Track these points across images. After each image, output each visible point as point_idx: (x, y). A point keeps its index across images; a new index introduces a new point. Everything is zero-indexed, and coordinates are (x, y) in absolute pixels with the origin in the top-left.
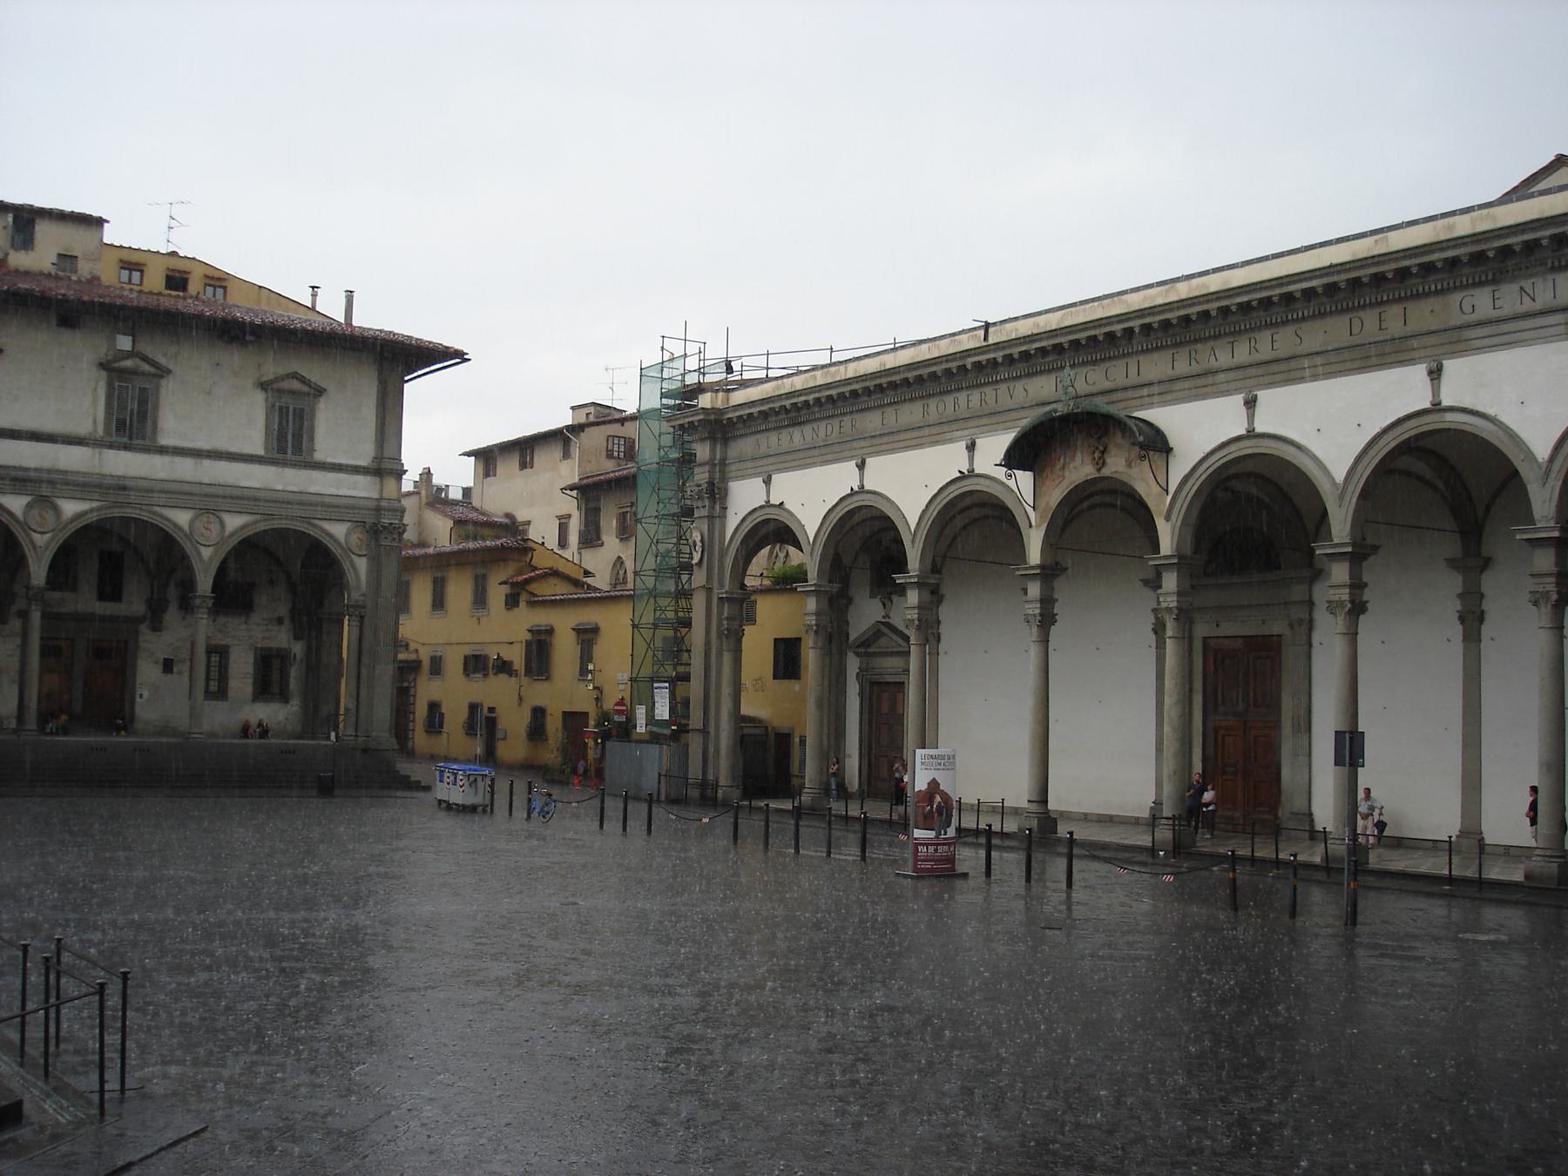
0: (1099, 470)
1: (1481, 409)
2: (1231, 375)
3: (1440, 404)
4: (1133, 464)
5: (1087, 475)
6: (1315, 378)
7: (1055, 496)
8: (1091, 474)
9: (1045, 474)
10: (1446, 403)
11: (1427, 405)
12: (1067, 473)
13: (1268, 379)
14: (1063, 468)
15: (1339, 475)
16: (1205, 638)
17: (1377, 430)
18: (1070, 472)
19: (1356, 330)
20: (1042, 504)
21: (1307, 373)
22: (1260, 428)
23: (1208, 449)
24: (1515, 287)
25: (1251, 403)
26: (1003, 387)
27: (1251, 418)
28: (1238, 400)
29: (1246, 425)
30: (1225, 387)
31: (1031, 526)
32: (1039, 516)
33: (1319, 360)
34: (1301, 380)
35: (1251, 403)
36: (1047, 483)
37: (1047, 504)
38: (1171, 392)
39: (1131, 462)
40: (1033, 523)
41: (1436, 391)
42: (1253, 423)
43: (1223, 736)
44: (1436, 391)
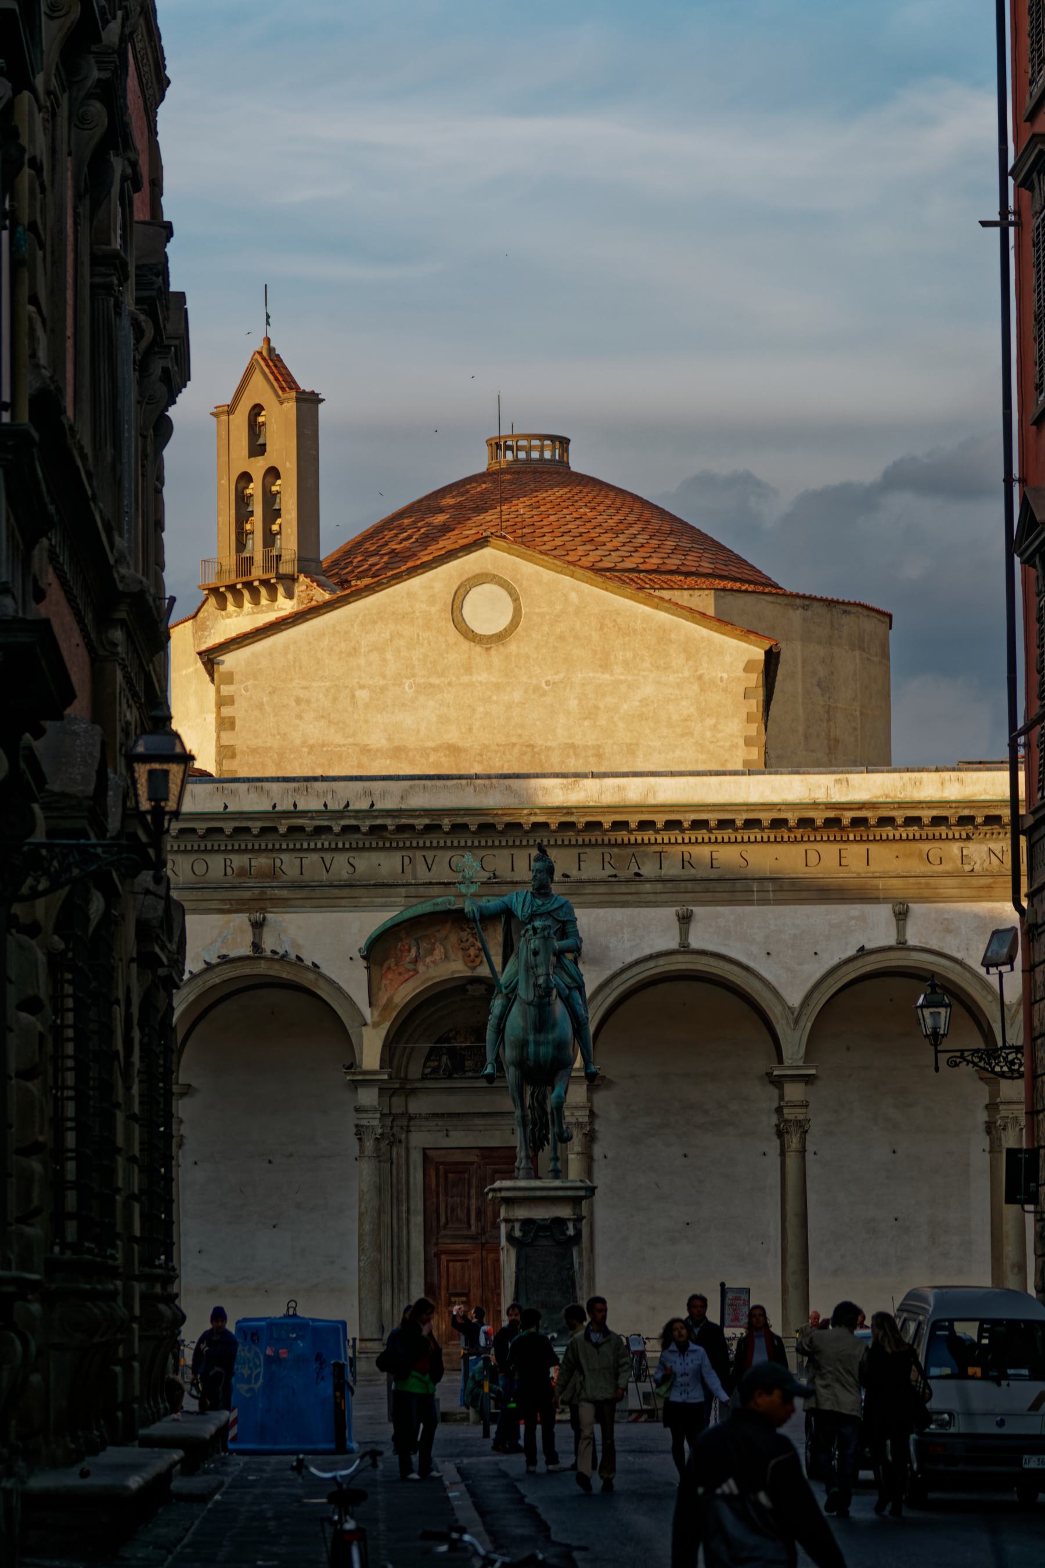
0: (474, 969)
1: (946, 951)
2: (659, 887)
3: (905, 943)
5: (453, 972)
6: (764, 902)
7: (404, 992)
8: (459, 972)
9: (386, 966)
10: (912, 942)
11: (892, 941)
12: (421, 968)
13: (708, 896)
14: (415, 961)
15: (794, 999)
16: (424, 1149)
17: (835, 961)
18: (428, 967)
19: (813, 858)
20: (383, 999)
21: (755, 896)
22: (695, 943)
23: (630, 959)
24: (984, 848)
25: (685, 920)
26: (315, 857)
27: (684, 934)
28: (669, 914)
29: (678, 940)
30: (651, 898)
31: (365, 1024)
32: (376, 1014)
33: (770, 886)
34: (749, 902)
35: (685, 920)
36: (390, 976)
37: (390, 1000)
38: (579, 894)
40: (369, 1020)
41: (901, 930)
42: (687, 938)
43: (448, 1261)
44: (901, 930)
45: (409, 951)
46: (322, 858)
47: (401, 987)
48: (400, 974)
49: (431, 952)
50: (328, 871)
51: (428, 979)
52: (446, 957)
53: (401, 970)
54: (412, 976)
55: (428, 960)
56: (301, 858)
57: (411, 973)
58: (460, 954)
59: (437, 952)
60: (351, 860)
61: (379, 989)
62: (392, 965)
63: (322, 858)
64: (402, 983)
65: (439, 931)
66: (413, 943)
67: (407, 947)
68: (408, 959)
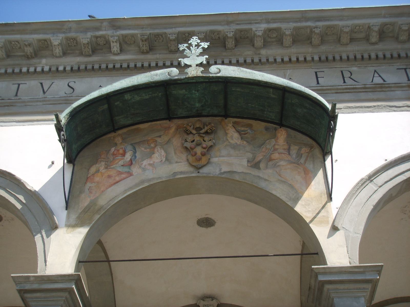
4: (262, 165)
8: (181, 173)
9: (93, 170)
12: (135, 170)
14: (131, 163)
18: (144, 169)
37: (93, 203)
39: (259, 162)
45: (124, 155)
46: (41, 84)
47: (109, 190)
48: (109, 177)
49: (150, 155)
50: (44, 92)
51: (143, 182)
52: (167, 159)
53: (112, 173)
54: (124, 179)
55: (145, 163)
56: (19, 85)
57: (123, 176)
58: (184, 156)
59: (156, 155)
60: (71, 84)
61: (81, 192)
62: (102, 169)
63: (41, 84)
64: (110, 186)
65: (160, 137)
66: (129, 148)
67: (121, 151)
68: (121, 163)
